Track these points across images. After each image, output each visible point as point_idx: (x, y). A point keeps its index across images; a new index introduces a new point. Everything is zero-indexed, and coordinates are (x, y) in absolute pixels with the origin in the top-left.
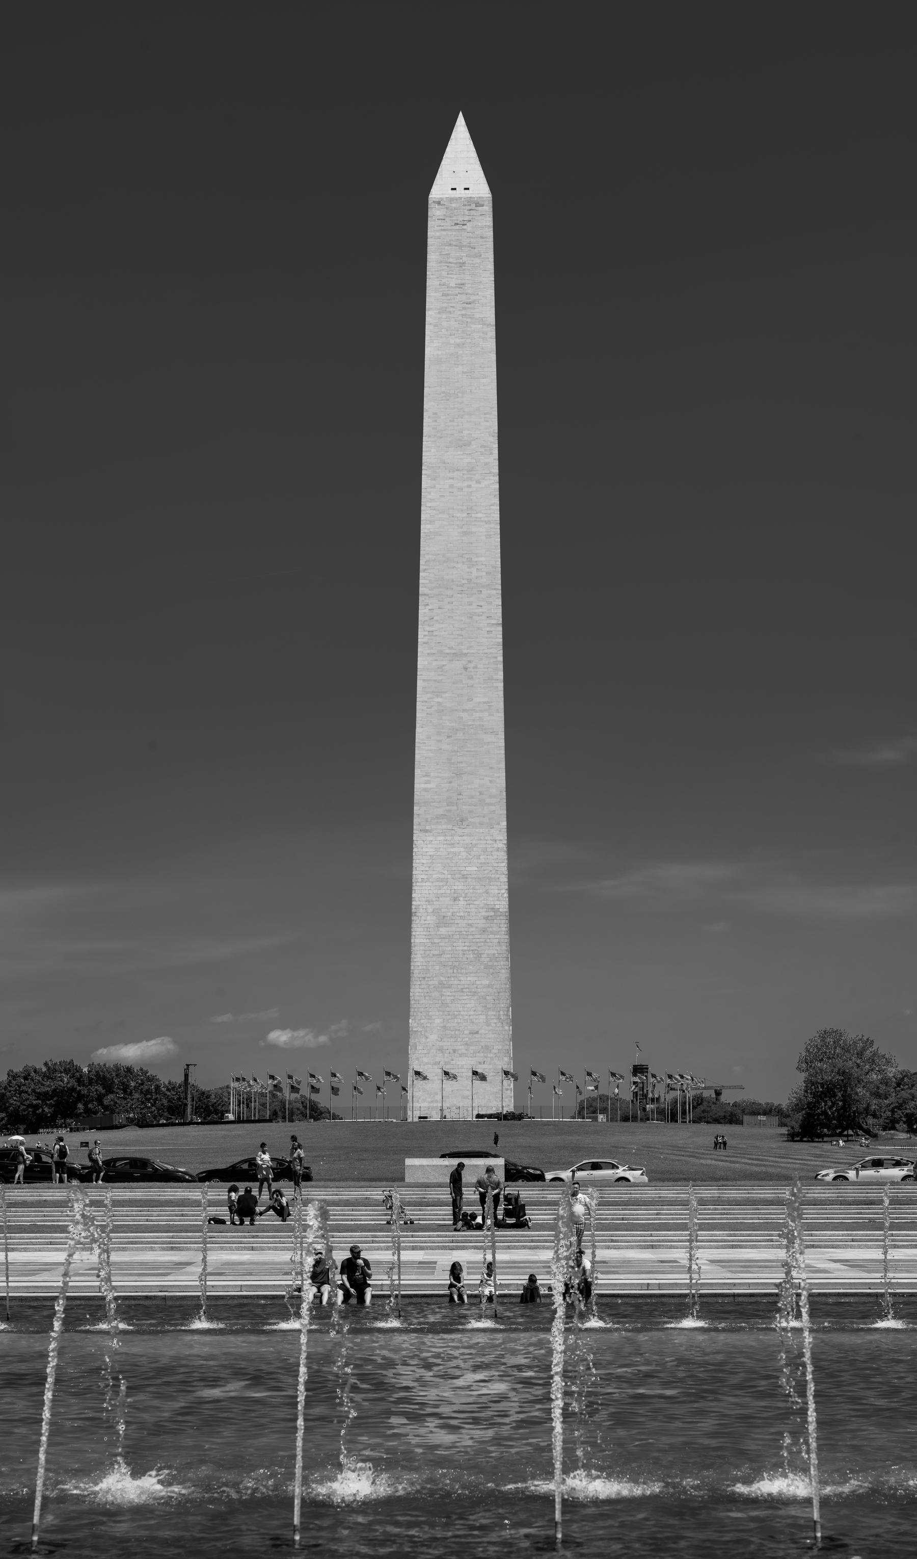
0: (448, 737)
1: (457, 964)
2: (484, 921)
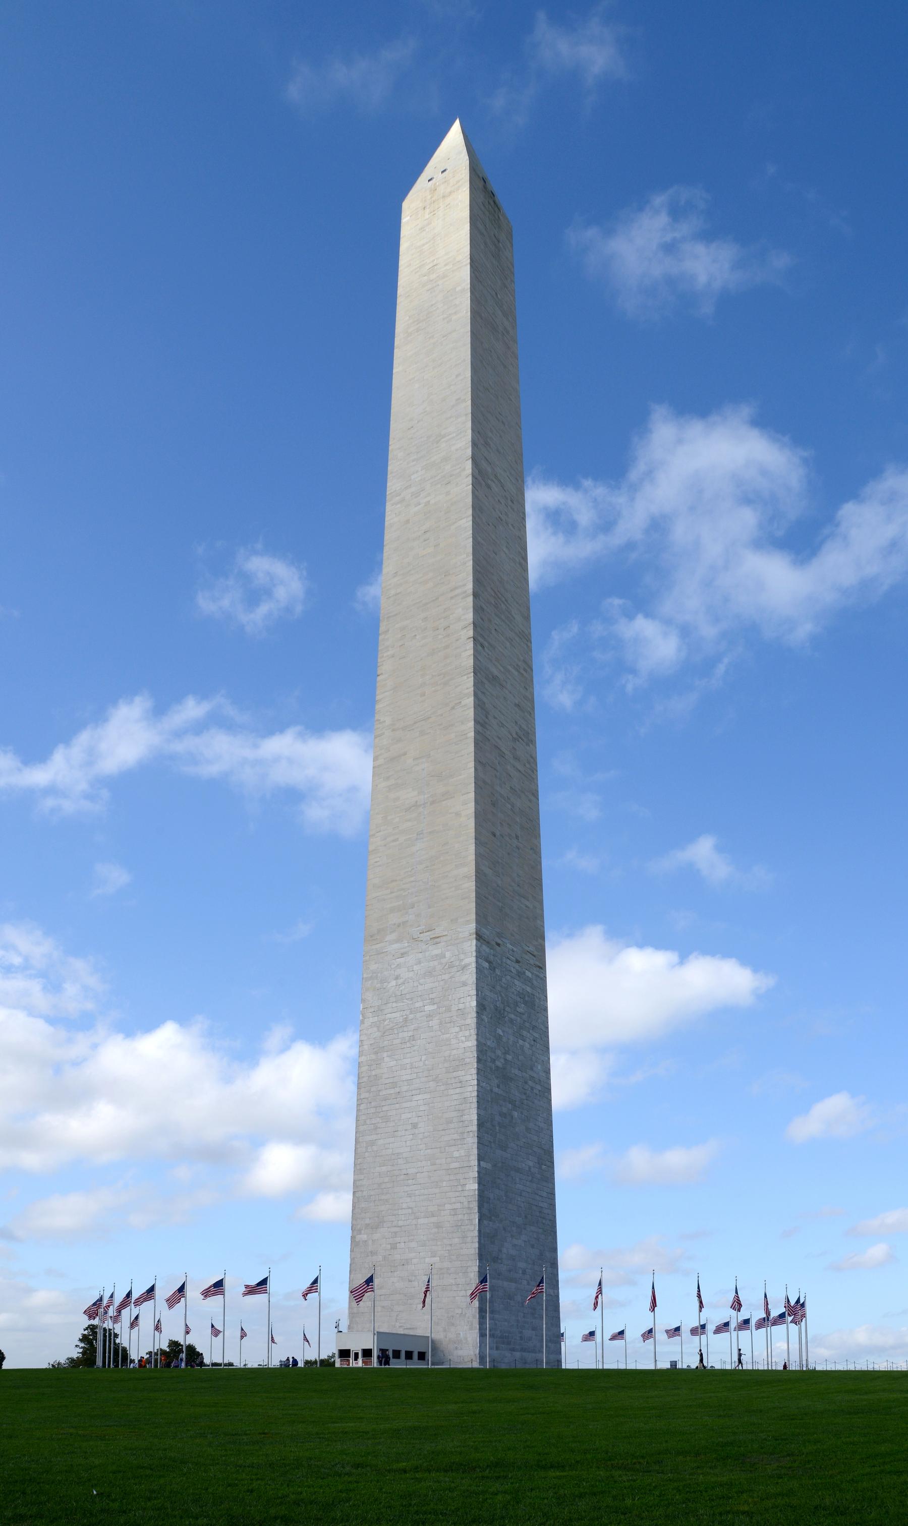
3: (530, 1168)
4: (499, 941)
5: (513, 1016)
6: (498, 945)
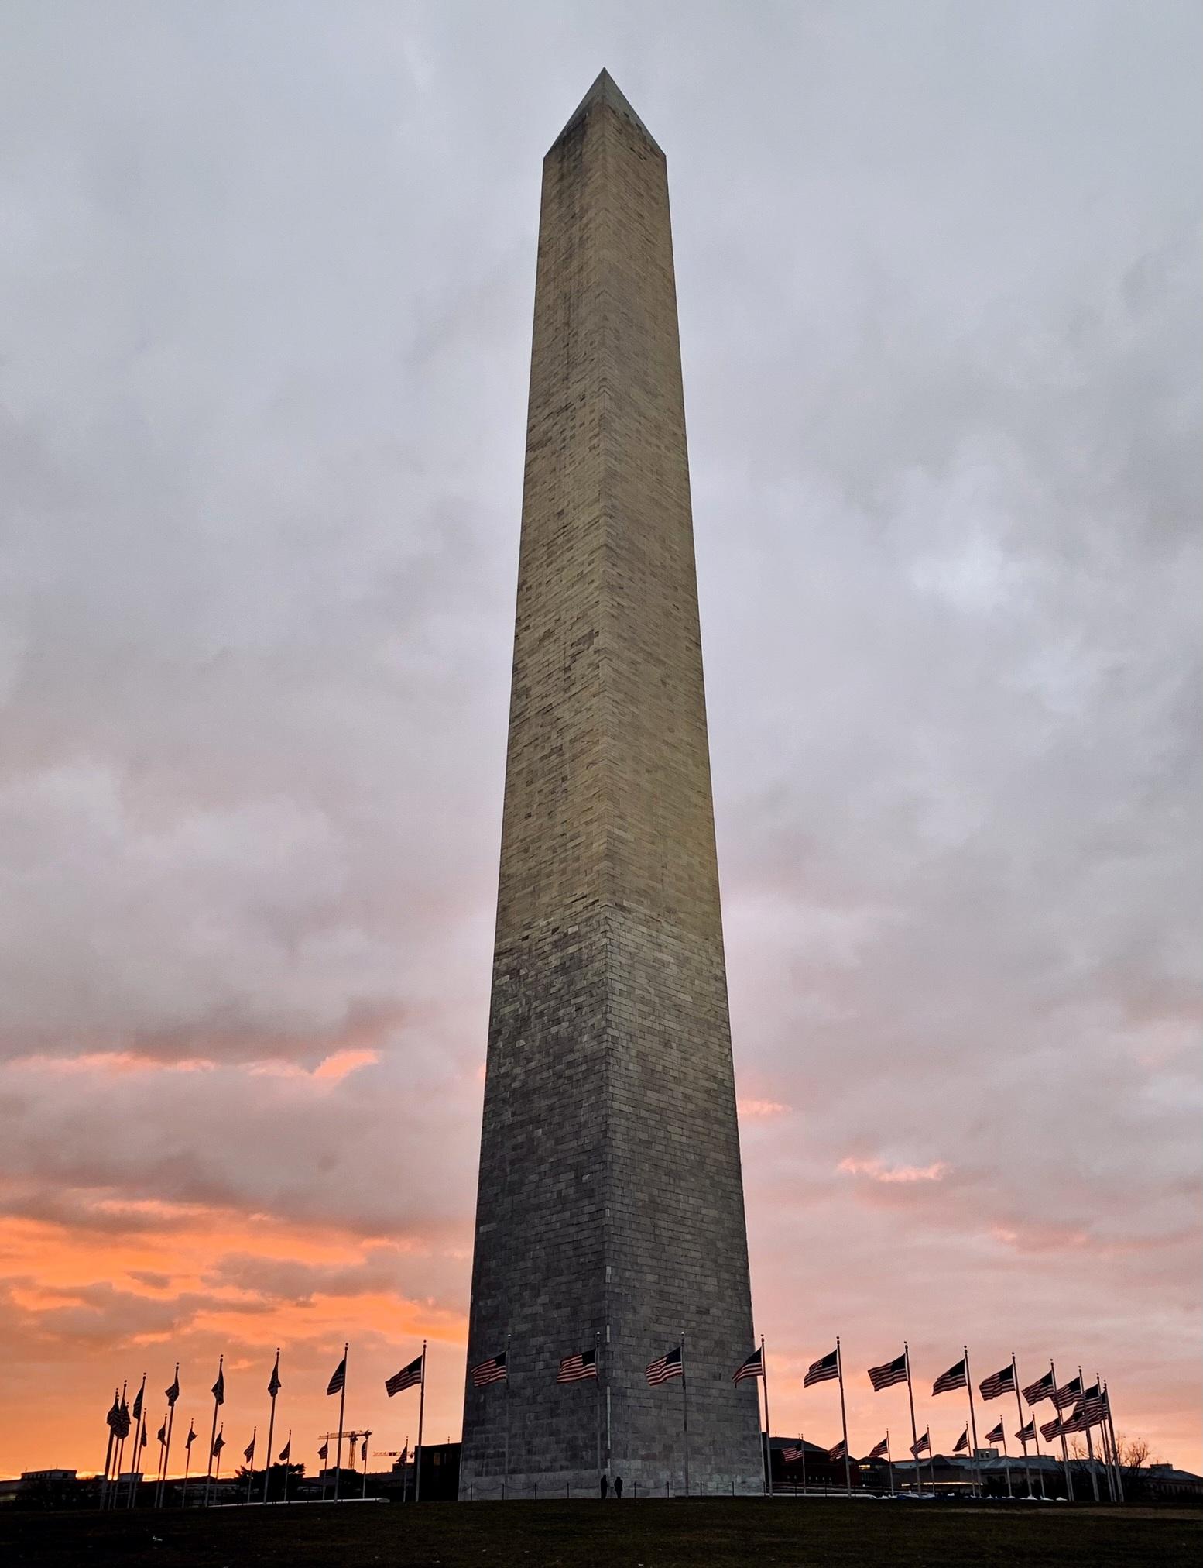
0: (648, 771)
1: (673, 1167)
2: (705, 1096)
3: (559, 1192)
4: (526, 933)
5: (543, 1007)
6: (527, 938)
